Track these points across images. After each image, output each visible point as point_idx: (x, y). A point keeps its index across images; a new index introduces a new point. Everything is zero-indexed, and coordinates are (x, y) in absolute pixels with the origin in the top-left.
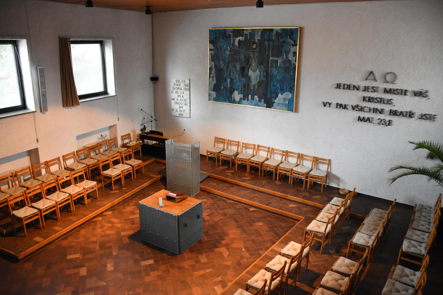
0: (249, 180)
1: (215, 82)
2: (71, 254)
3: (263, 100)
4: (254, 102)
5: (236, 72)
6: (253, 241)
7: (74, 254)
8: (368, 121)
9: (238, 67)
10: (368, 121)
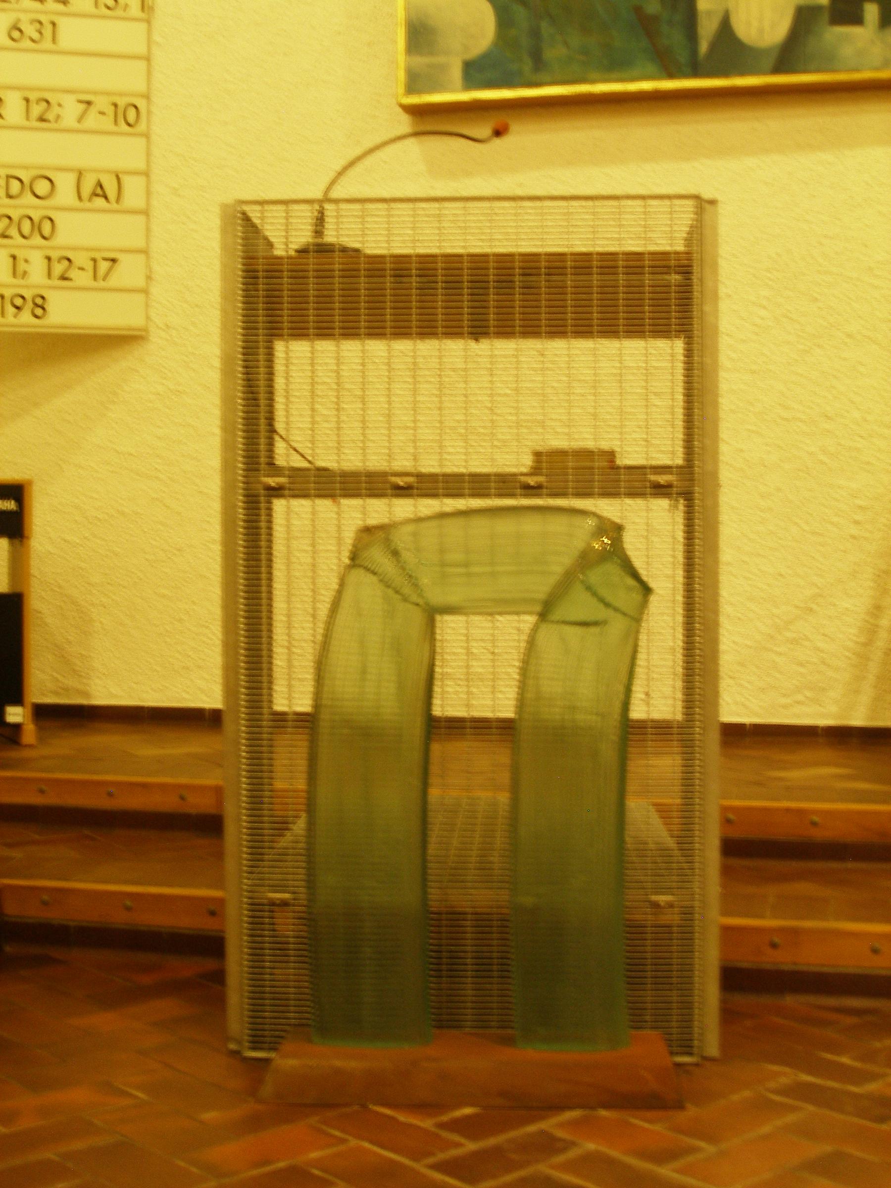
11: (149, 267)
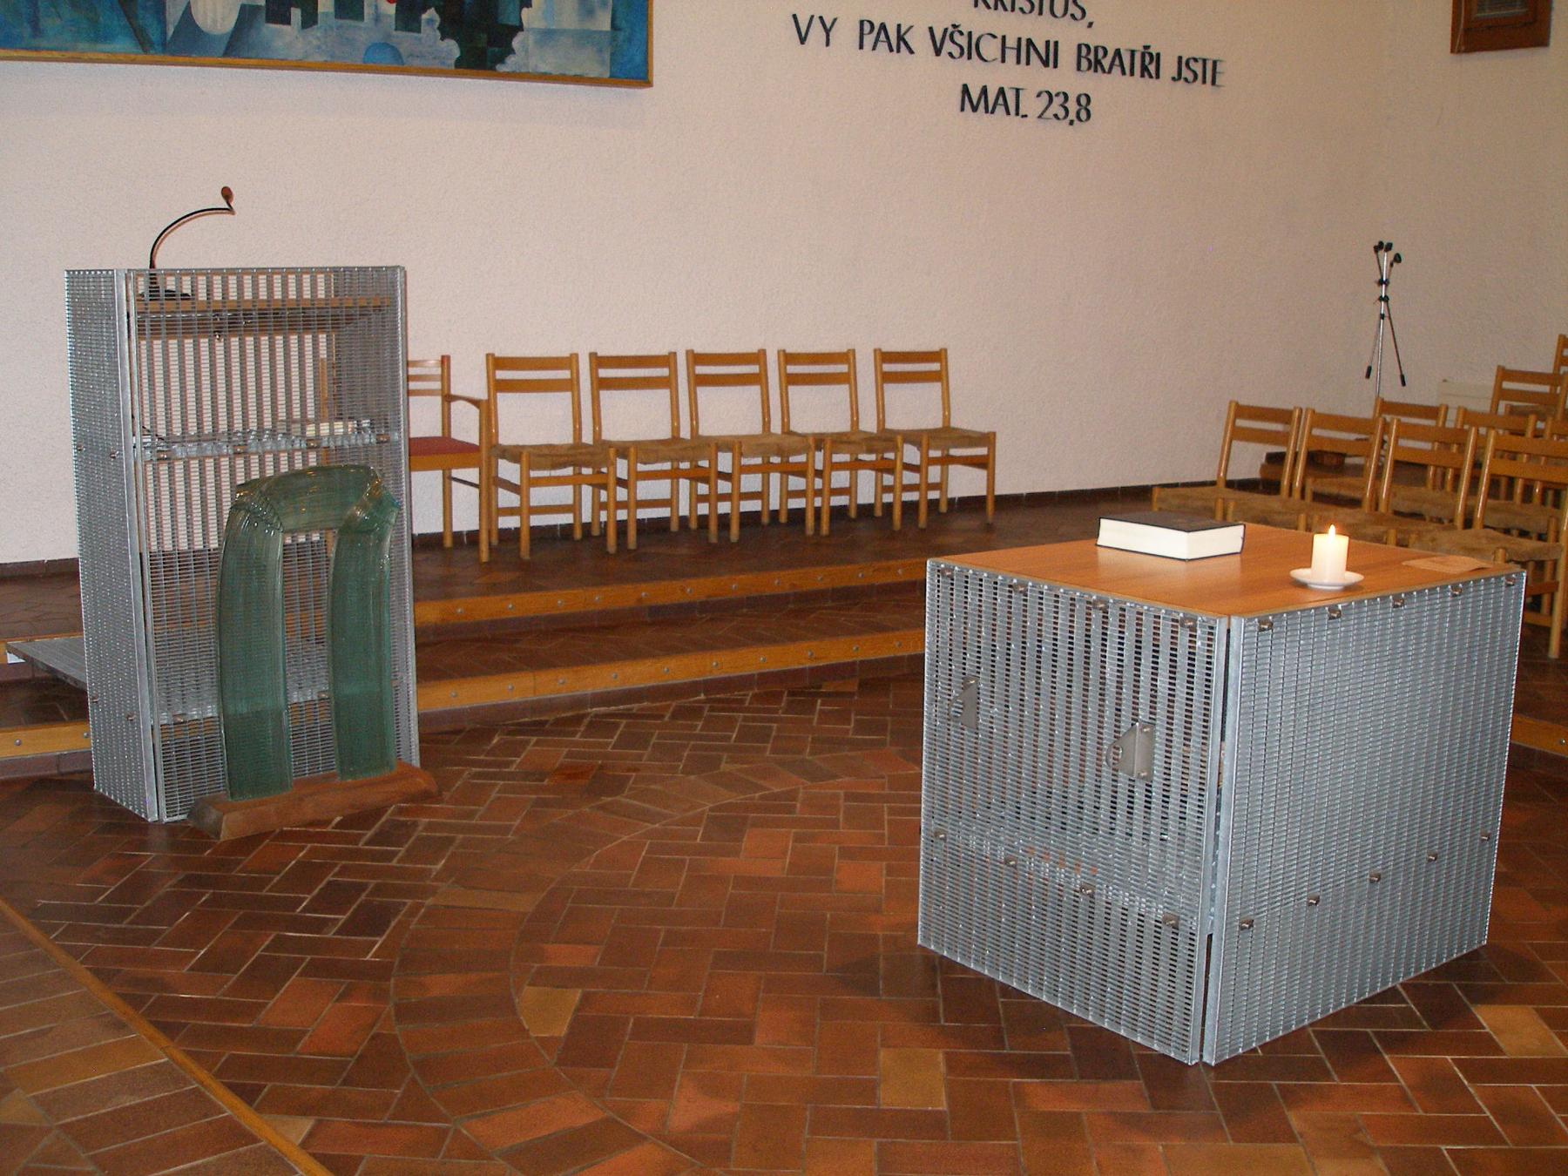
3: (430, 14)
4: (363, 32)
8: (1000, 110)
10: (1000, 110)
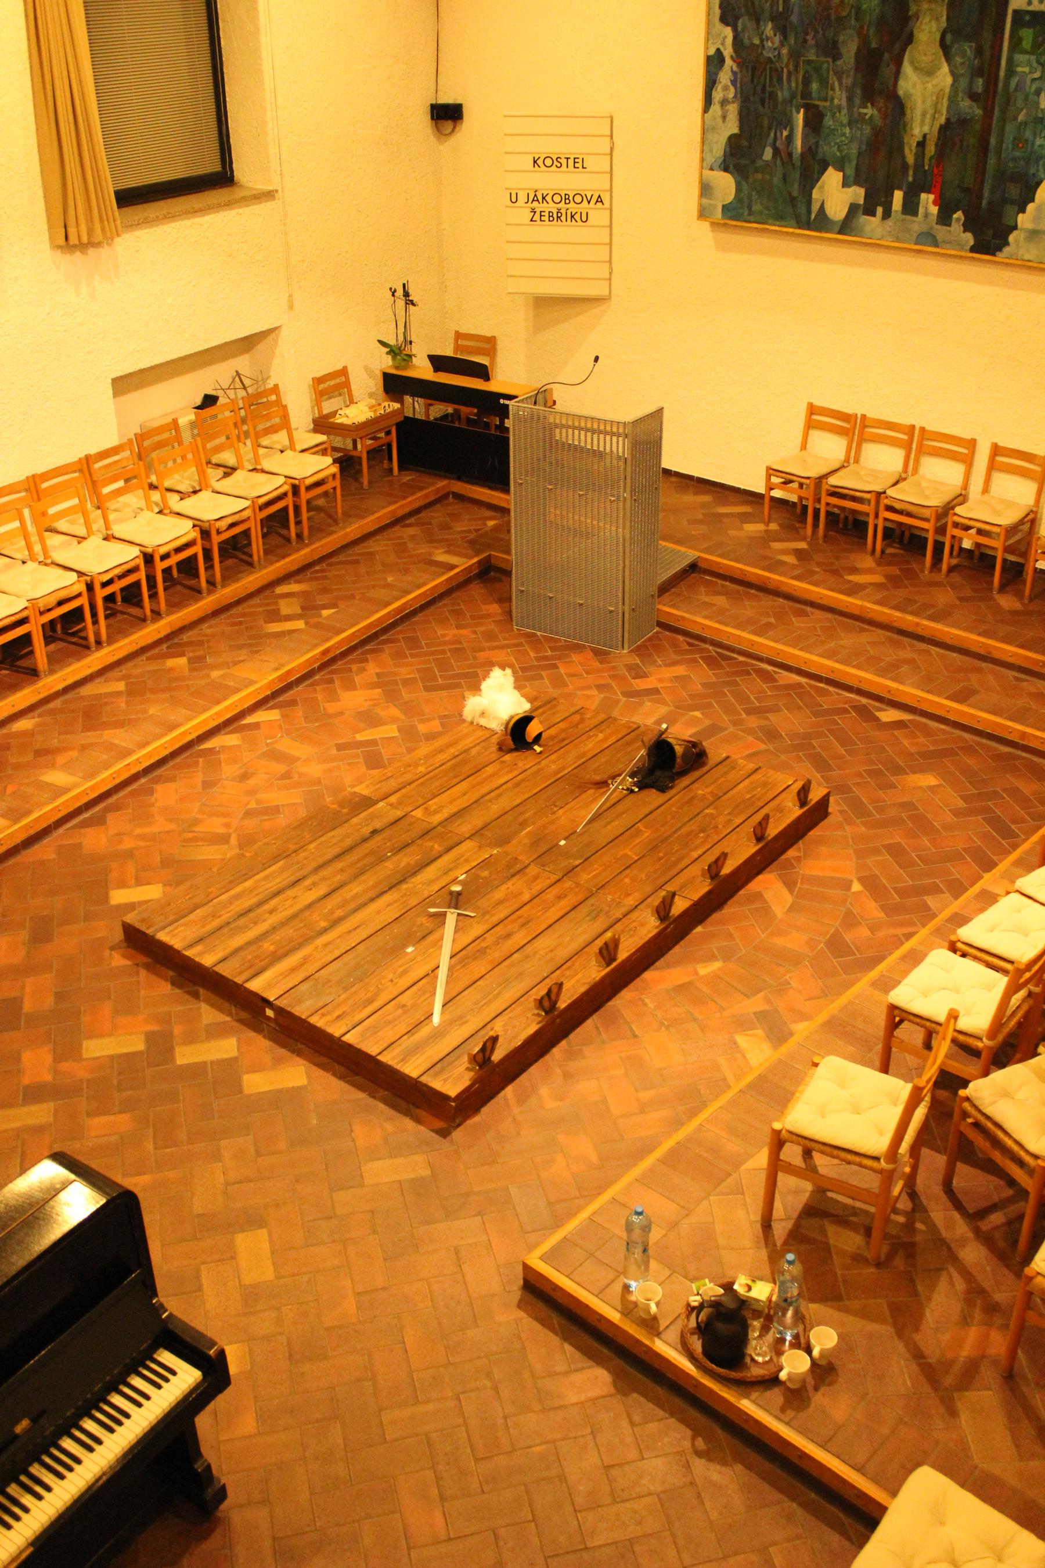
0: (878, 586)
1: (732, 127)
2: (123, 884)
3: (959, 215)
4: (917, 224)
5: (839, 75)
6: (895, 851)
7: (139, 882)
9: (850, 49)
11: (611, 268)
